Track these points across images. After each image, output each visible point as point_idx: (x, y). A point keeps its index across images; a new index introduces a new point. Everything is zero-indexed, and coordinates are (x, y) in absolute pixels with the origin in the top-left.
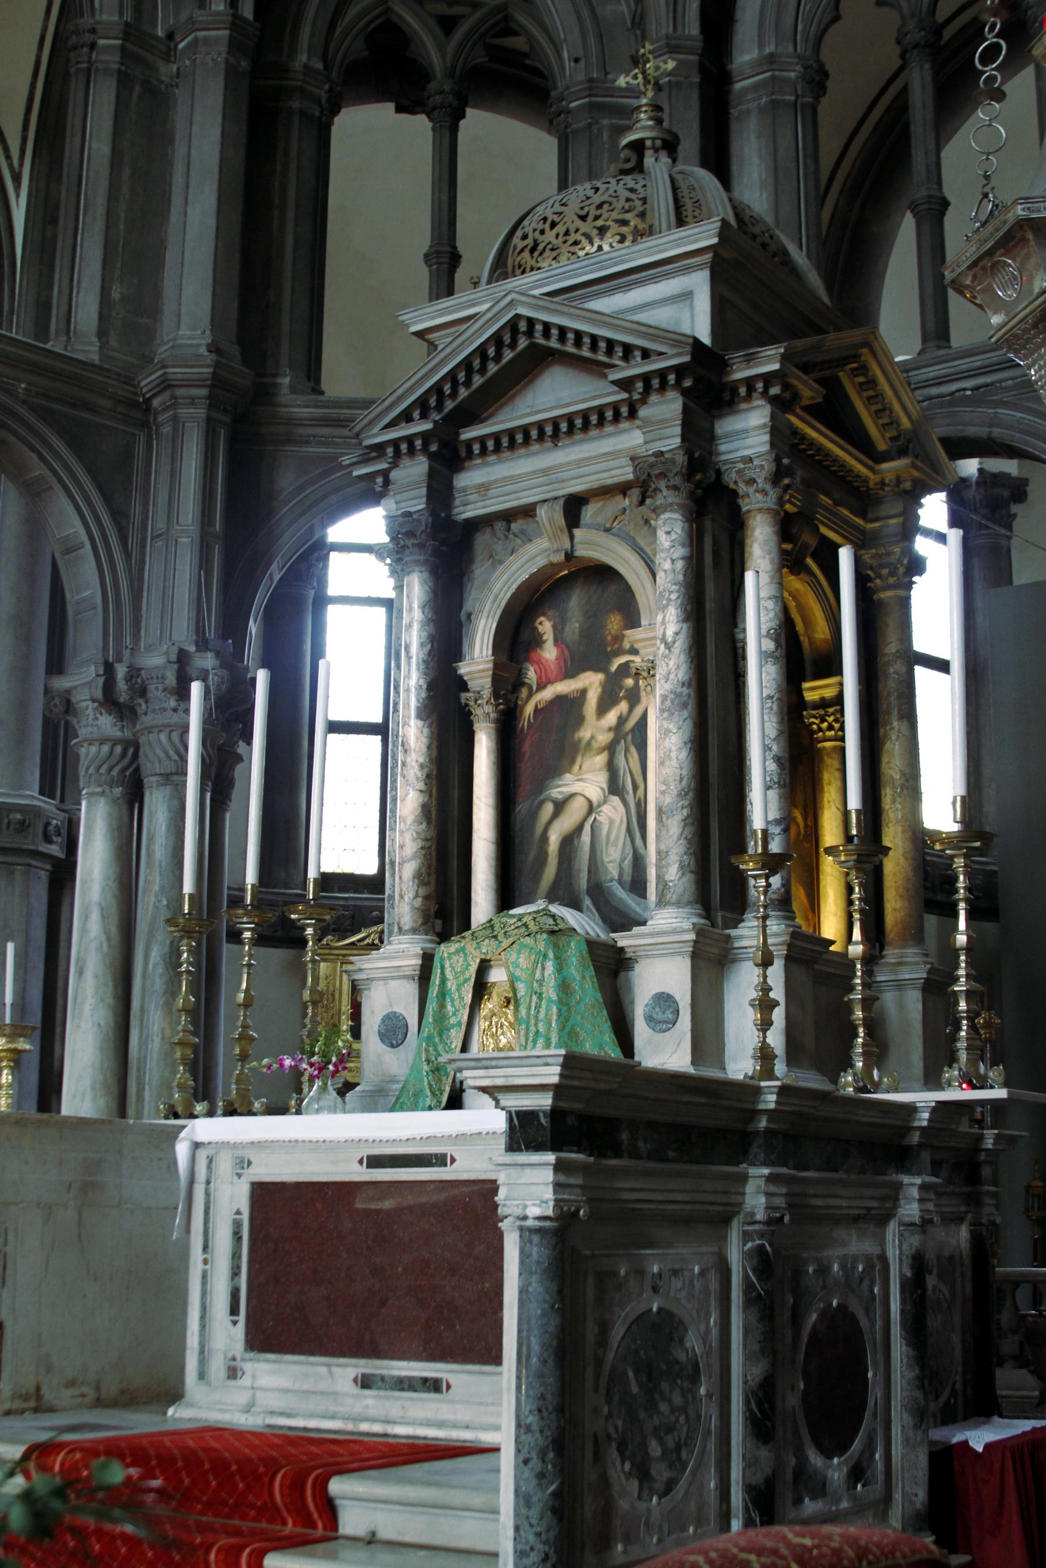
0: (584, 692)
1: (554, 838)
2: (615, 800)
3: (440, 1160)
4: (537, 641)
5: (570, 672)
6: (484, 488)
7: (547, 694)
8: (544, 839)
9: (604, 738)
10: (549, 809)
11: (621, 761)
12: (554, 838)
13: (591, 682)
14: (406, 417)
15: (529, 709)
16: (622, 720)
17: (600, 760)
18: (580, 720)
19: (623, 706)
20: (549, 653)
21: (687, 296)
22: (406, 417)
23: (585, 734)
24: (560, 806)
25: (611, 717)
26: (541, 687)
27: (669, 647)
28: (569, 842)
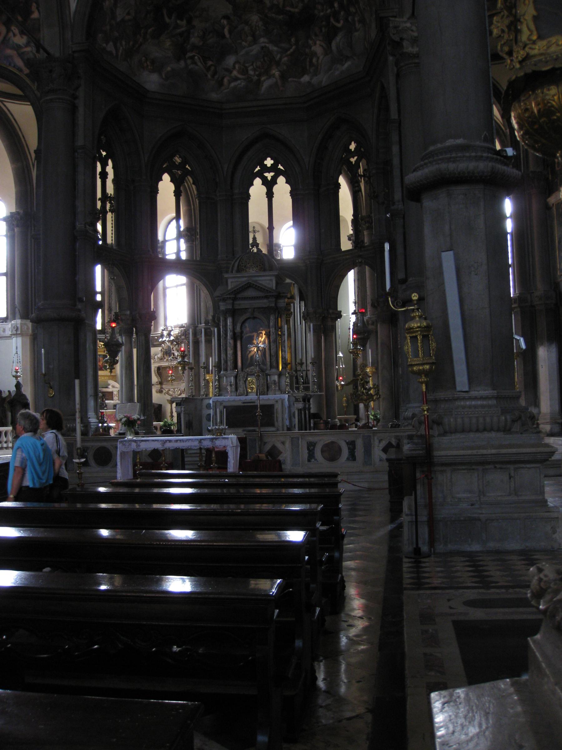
1: (249, 356)
3: (254, 402)
4: (246, 327)
10: (248, 352)
14: (229, 294)
15: (244, 337)
20: (248, 329)
21: (271, 280)
22: (229, 294)
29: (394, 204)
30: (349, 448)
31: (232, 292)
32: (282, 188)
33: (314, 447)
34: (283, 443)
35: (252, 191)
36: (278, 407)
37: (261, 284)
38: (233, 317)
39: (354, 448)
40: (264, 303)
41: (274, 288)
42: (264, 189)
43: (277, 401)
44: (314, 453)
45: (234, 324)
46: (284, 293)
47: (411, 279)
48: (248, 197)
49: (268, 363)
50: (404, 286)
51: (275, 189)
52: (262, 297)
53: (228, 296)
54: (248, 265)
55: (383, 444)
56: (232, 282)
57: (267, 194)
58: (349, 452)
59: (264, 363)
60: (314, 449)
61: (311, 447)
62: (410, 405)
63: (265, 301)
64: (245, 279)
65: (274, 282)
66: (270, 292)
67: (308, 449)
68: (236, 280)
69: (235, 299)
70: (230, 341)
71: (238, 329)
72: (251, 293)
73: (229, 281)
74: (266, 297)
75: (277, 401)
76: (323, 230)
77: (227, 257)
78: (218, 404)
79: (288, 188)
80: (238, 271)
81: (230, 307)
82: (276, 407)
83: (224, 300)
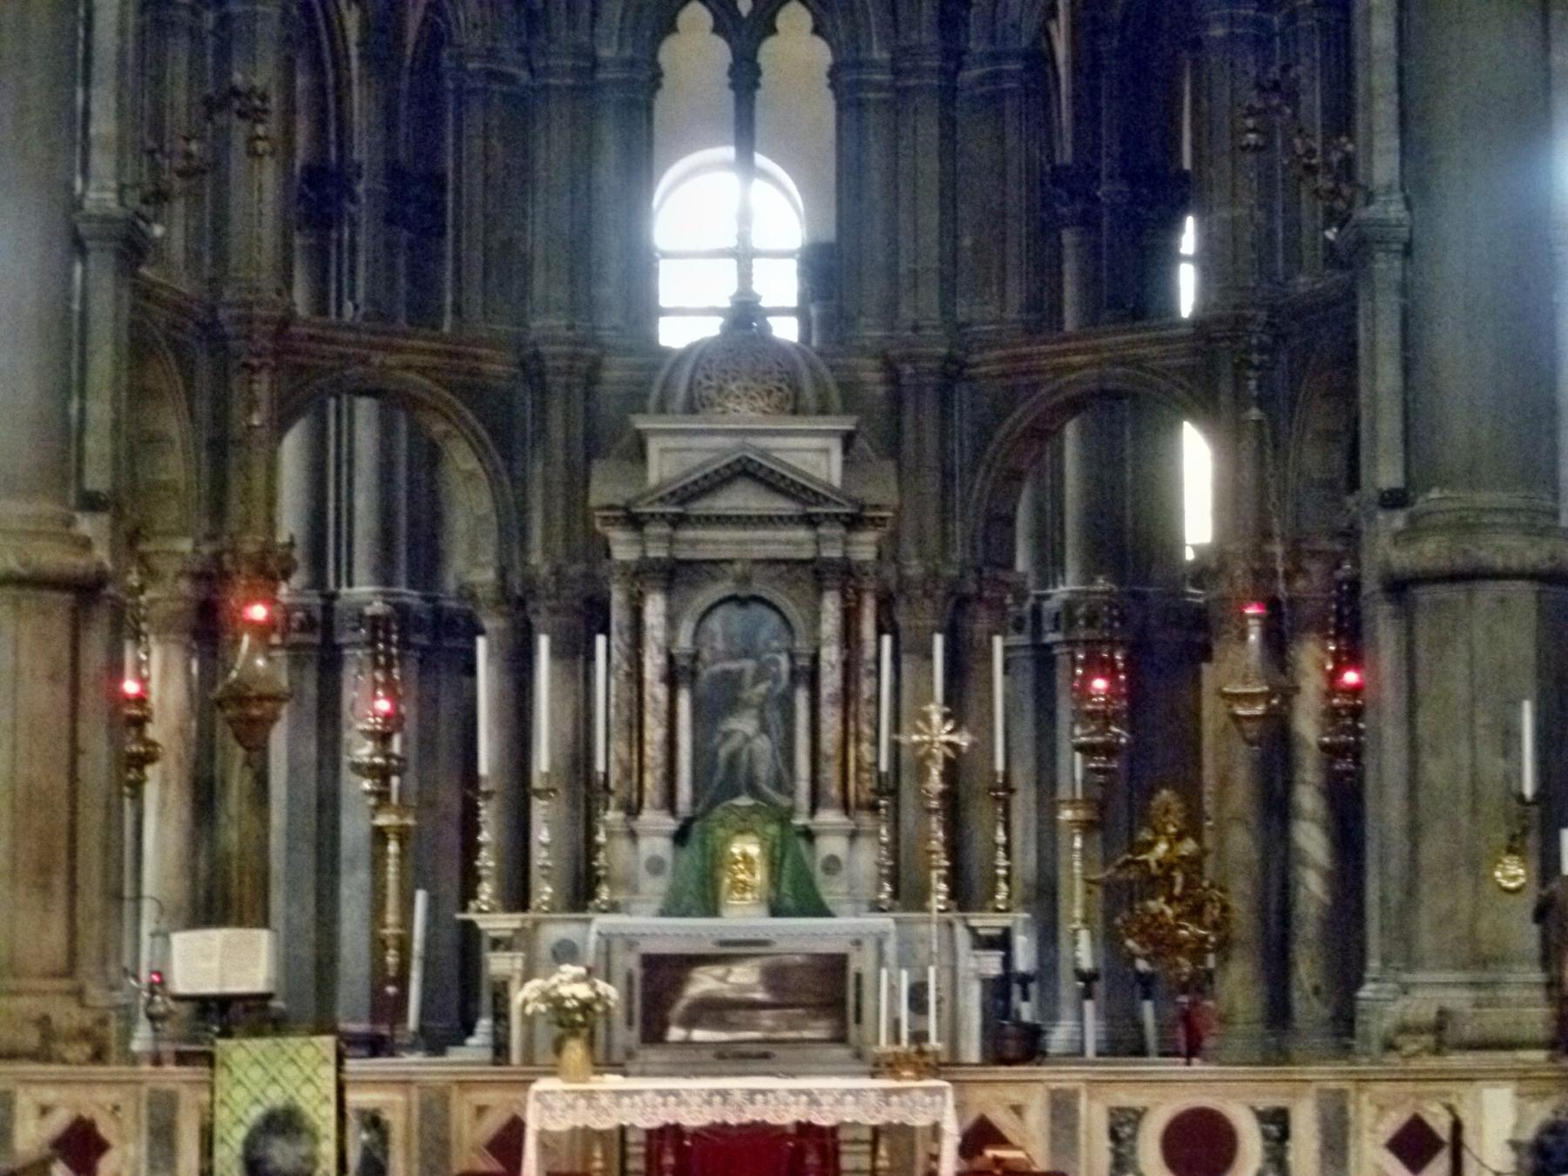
0: (741, 672)
1: (723, 753)
2: (765, 737)
5: (732, 656)
6: (694, 543)
7: (717, 668)
8: (715, 755)
9: (756, 700)
10: (717, 739)
11: (768, 715)
12: (723, 753)
13: (749, 665)
14: (661, 499)
16: (770, 690)
17: (754, 712)
18: (741, 688)
19: (769, 683)
21: (826, 451)
22: (661, 499)
23: (745, 695)
24: (727, 736)
25: (762, 688)
26: (714, 663)
27: (833, 667)
28: (733, 757)
29: (1370, 198)
30: (1266, 1135)
31: (673, 494)
32: (797, 50)
33: (1136, 1129)
34: (1017, 1110)
35: (671, 53)
36: (861, 962)
37: (782, 463)
38: (668, 590)
39: (1285, 1135)
40: (796, 542)
41: (836, 481)
42: (720, 52)
43: (858, 943)
44: (1133, 1150)
45: (672, 621)
46: (877, 507)
47: (1435, 494)
48: (656, 78)
49: (803, 787)
50: (1399, 520)
51: (770, 52)
52: (791, 518)
53: (658, 509)
54: (733, 387)
55: (1393, 1122)
56: (664, 451)
57: (733, 72)
58: (1267, 1149)
59: (783, 782)
60: (1133, 1137)
61: (1123, 1126)
62: (1421, 977)
63: (802, 534)
64: (718, 441)
65: (837, 457)
66: (827, 499)
67: (1114, 1135)
68: (682, 442)
69: (679, 521)
70: (656, 690)
71: (684, 642)
72: (743, 498)
73: (654, 446)
74: (810, 521)
75: (858, 943)
76: (967, 242)
77: (570, 327)
78: (618, 945)
79: (820, 54)
80: (691, 408)
81: (657, 551)
82: (853, 966)
83: (634, 522)
